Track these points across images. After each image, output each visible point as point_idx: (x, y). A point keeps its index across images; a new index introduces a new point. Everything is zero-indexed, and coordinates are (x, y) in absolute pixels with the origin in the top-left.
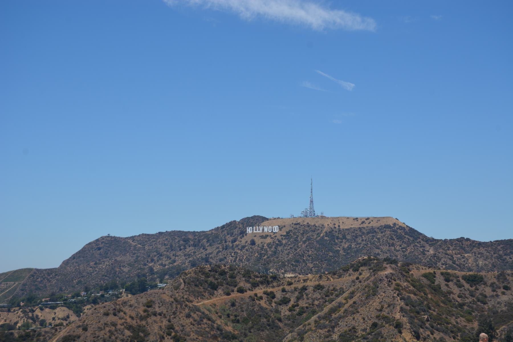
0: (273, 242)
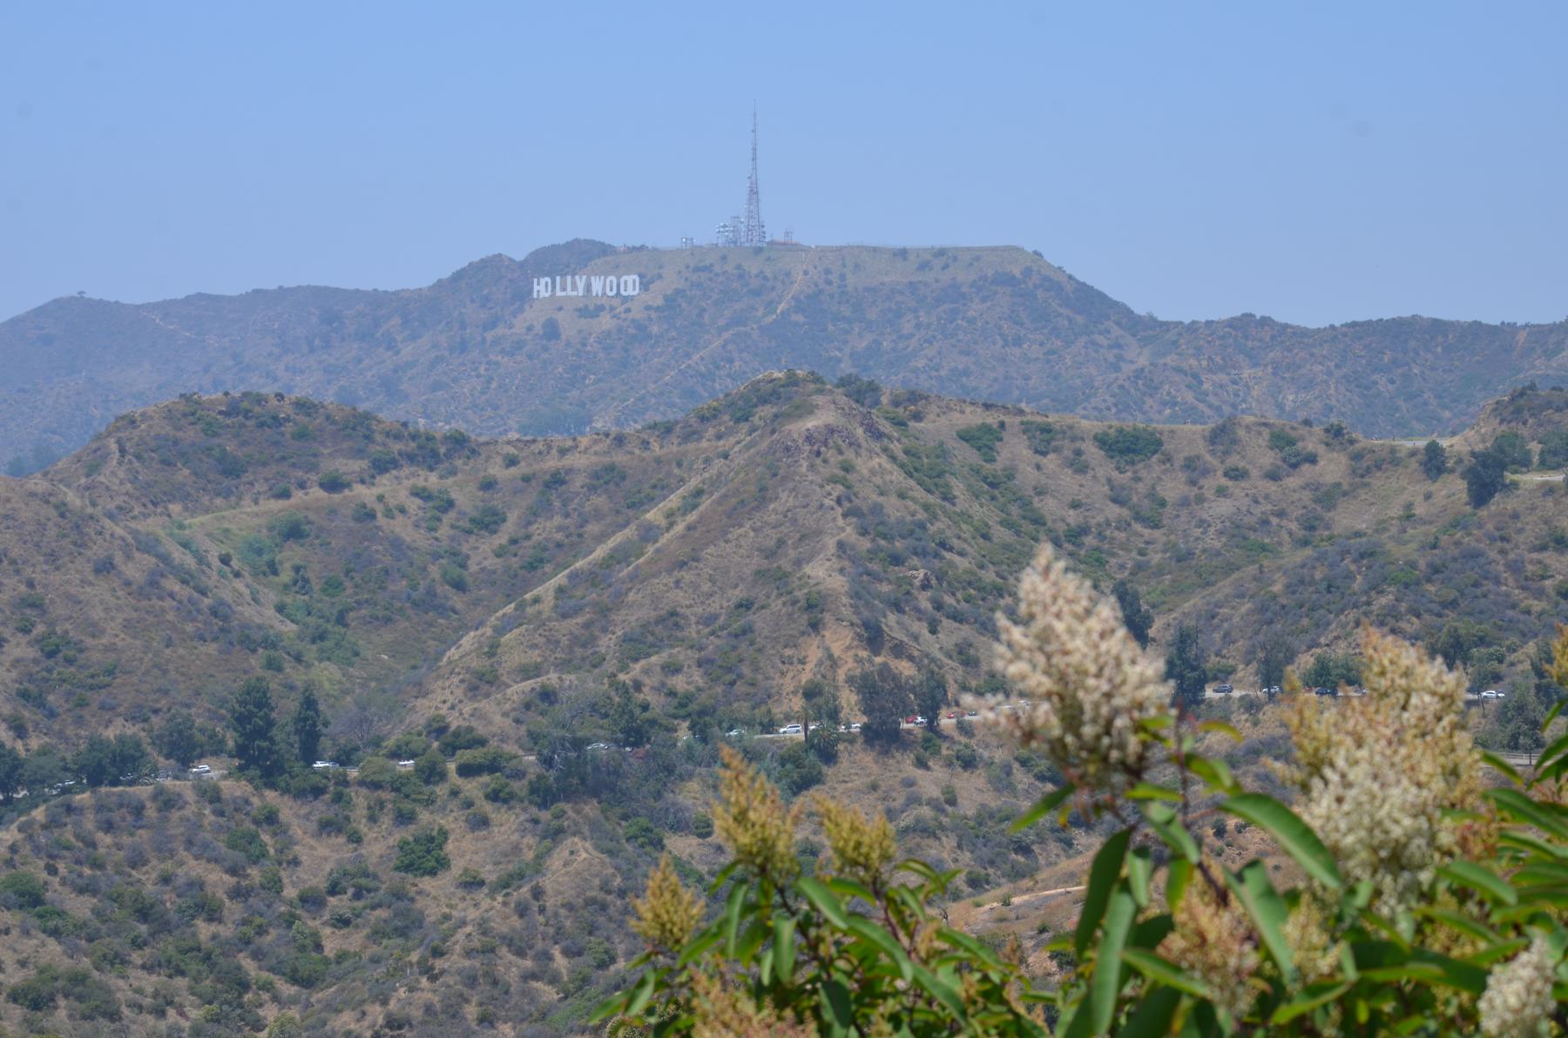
0: (620, 330)
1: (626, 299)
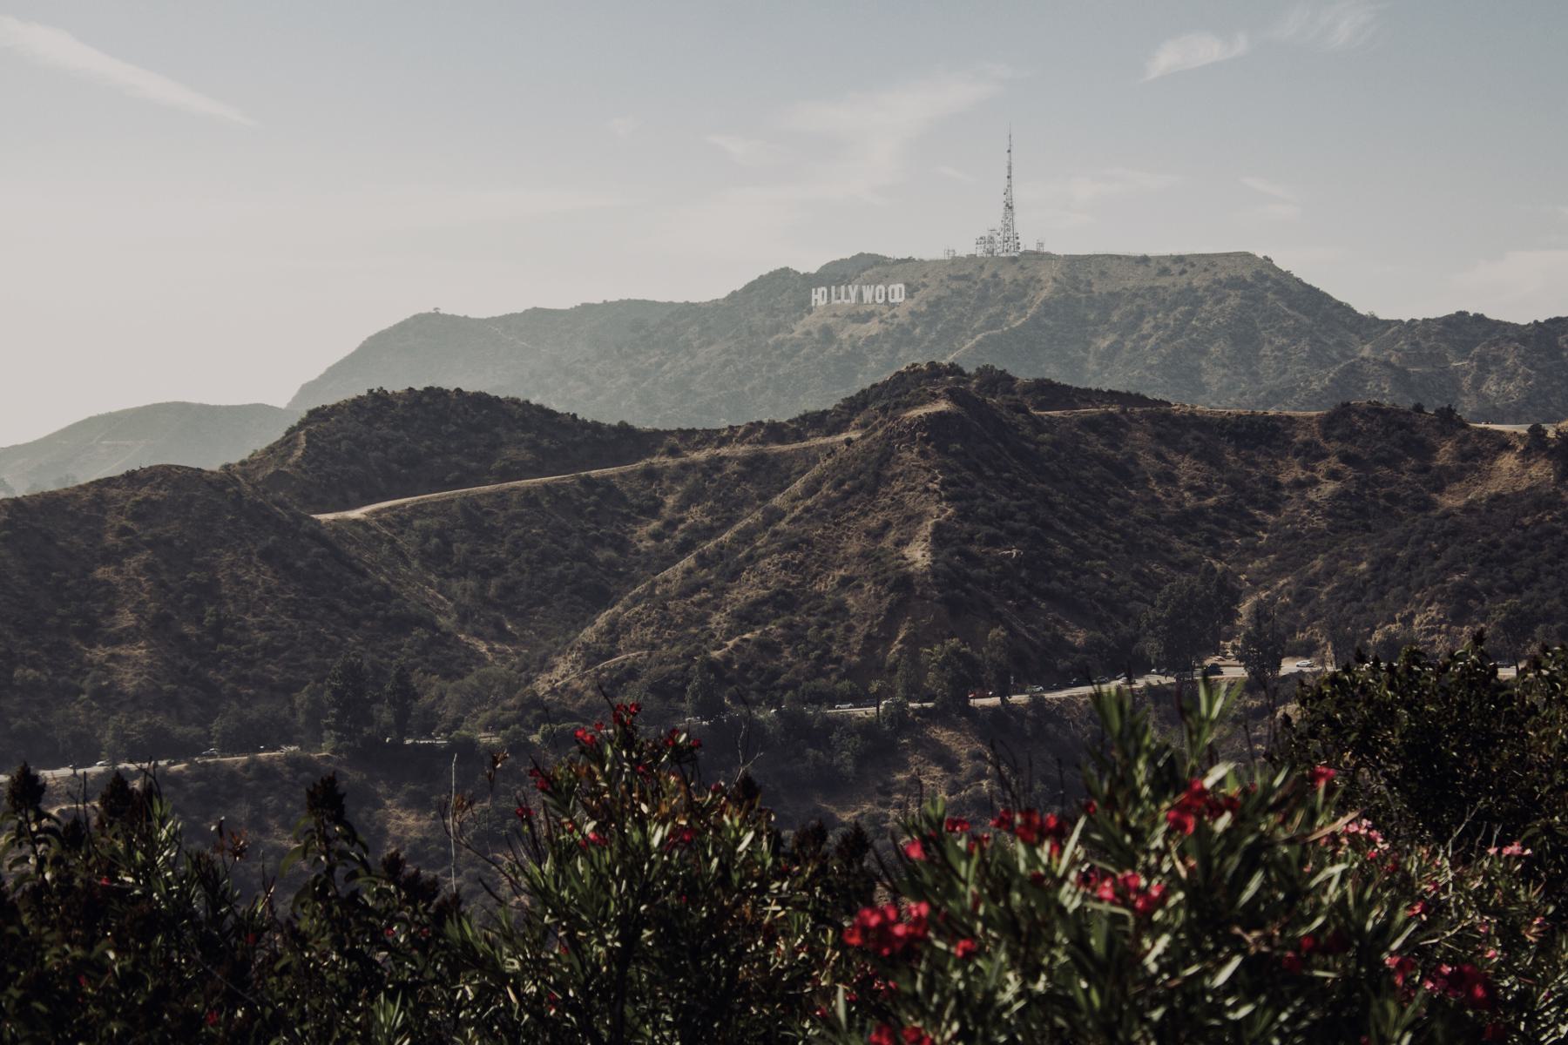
1: (894, 305)
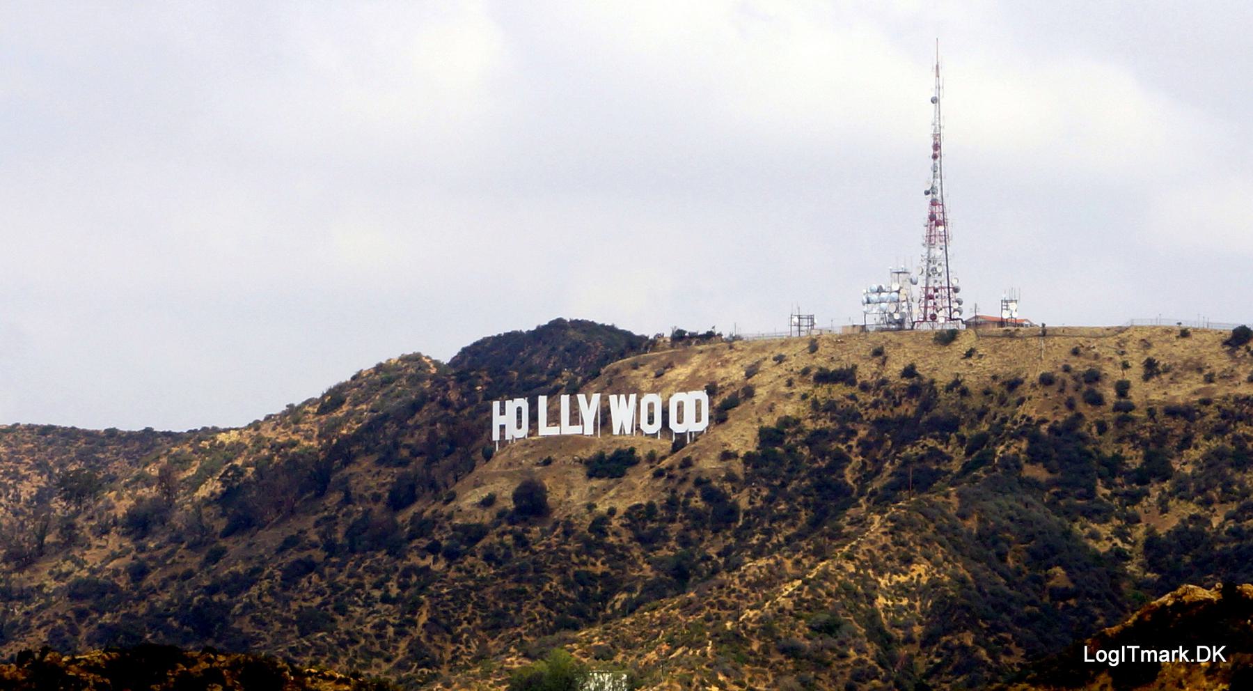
0: (671, 504)
1: (680, 442)
